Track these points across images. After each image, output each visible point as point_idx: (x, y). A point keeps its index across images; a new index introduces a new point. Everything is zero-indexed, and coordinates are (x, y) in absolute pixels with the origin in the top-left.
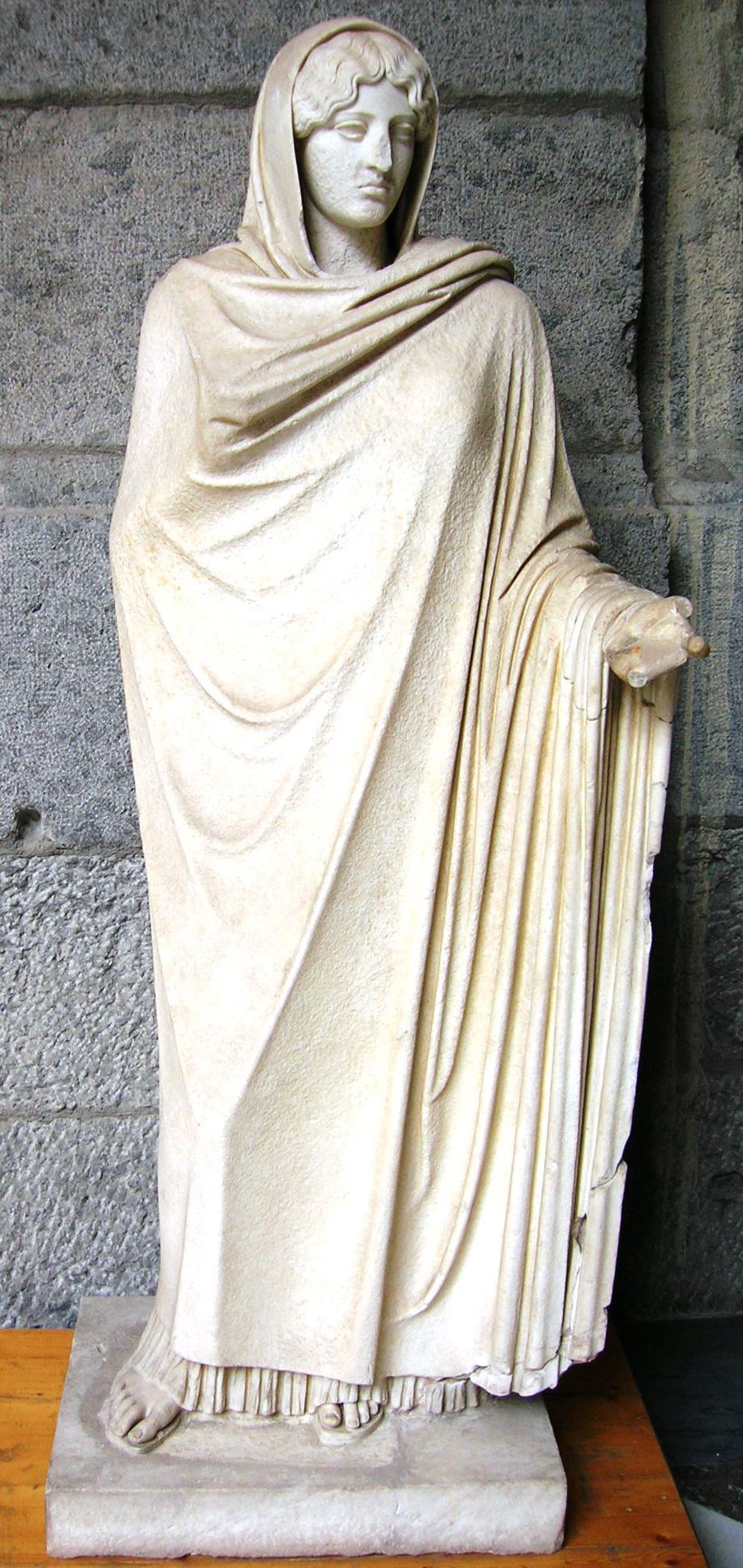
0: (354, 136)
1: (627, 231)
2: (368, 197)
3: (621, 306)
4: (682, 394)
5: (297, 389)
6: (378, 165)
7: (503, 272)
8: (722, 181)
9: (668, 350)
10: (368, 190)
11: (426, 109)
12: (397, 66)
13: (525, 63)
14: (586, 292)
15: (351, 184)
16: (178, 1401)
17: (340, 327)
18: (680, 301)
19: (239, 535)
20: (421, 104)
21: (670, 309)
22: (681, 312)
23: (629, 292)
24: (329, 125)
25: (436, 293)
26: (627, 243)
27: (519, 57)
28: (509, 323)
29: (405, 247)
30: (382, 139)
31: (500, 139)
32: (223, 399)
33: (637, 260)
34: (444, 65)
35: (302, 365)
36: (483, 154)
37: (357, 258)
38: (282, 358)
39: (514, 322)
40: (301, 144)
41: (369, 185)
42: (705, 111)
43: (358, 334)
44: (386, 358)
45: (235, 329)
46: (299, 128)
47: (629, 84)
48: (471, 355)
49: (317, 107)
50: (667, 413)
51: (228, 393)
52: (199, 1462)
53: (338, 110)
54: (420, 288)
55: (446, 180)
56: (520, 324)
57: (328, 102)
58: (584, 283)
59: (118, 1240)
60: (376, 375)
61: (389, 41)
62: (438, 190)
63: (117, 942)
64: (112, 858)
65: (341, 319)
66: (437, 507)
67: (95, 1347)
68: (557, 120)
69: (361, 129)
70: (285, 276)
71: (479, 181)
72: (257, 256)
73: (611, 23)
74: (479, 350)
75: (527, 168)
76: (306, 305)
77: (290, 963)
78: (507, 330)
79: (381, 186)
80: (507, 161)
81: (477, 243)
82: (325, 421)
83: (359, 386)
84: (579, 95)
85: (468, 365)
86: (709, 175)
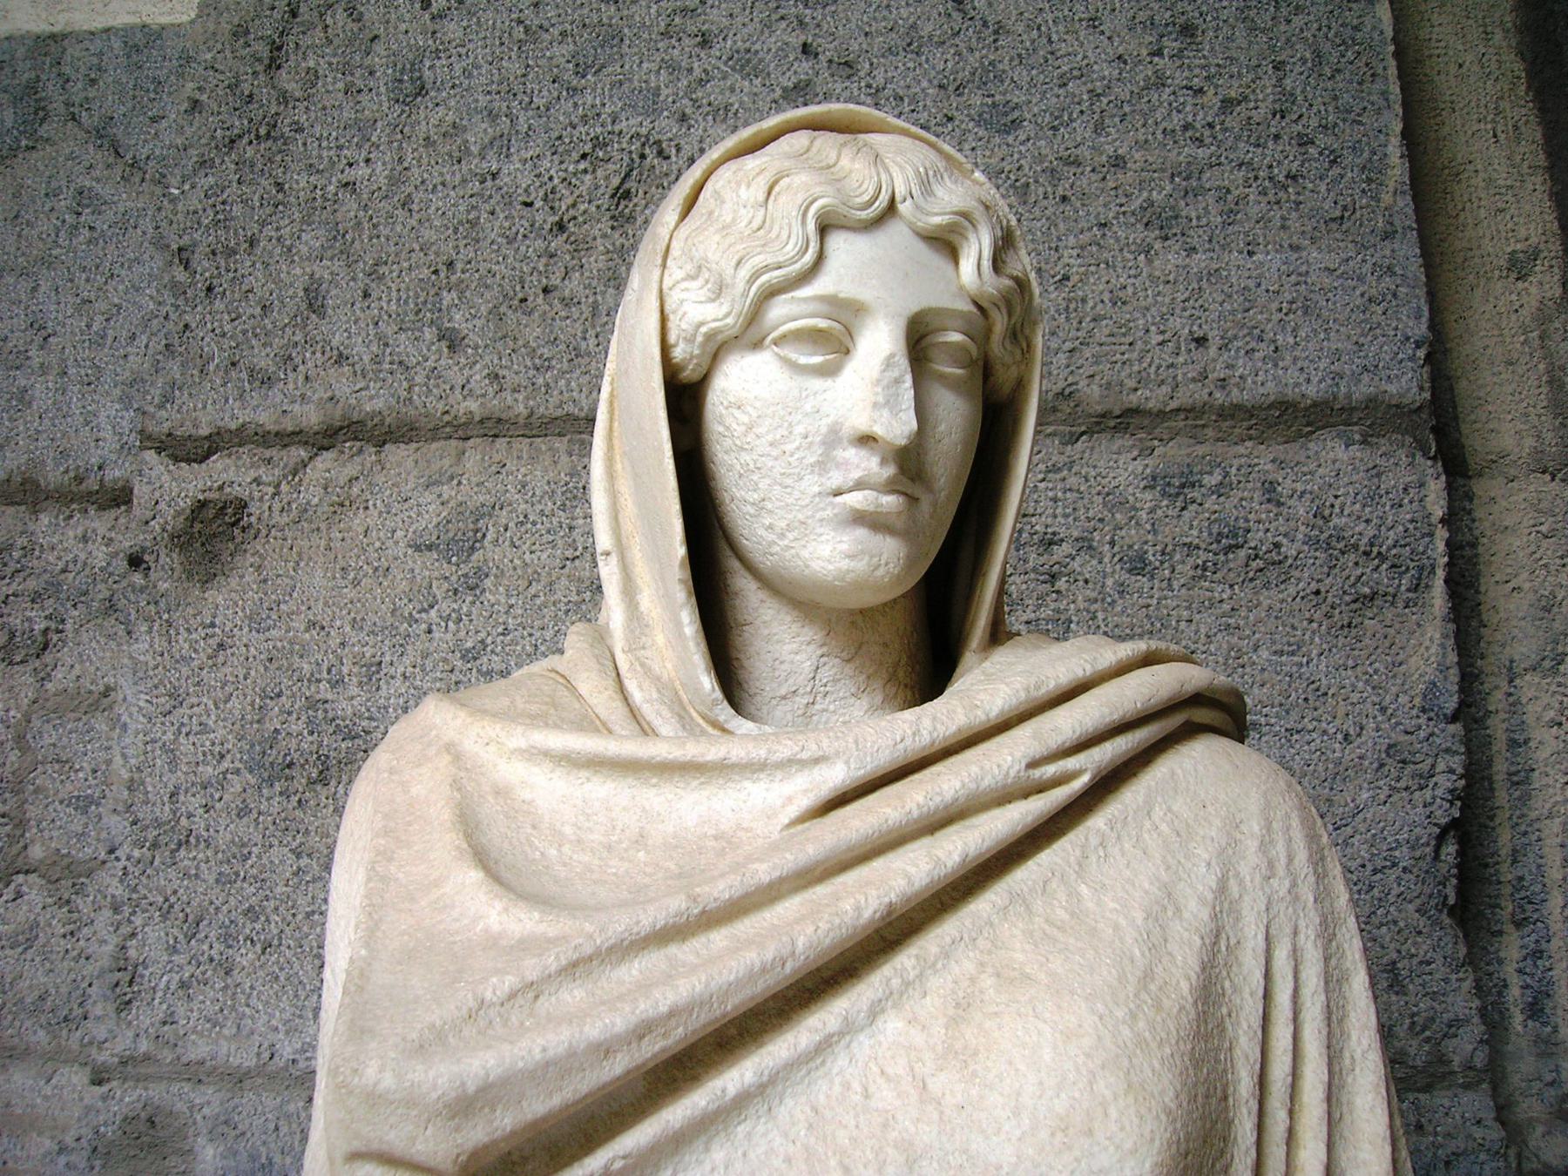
0: (817, 359)
1: (1427, 647)
2: (860, 518)
3: (1428, 793)
4: (1538, 954)
5: (618, 1066)
6: (878, 430)
7: (1215, 714)
9: (1507, 873)
10: (856, 499)
11: (1007, 301)
12: (926, 186)
13: (1213, 351)
14: (1359, 769)
15: (812, 485)
17: (764, 872)
18: (1520, 780)
20: (993, 285)
21: (1502, 796)
22: (1525, 798)
23: (1441, 766)
24: (748, 333)
25: (1050, 770)
26: (1430, 672)
27: (1201, 341)
28: (1252, 845)
29: (969, 658)
30: (889, 363)
31: (1177, 488)
33: (1451, 704)
34: (1062, 358)
35: (644, 987)
36: (1143, 515)
37: (845, 688)
38: (575, 968)
39: (1265, 846)
40: (685, 400)
41: (859, 485)
42: (1529, 442)
43: (821, 891)
44: (905, 961)
45: (475, 875)
46: (678, 353)
47: (1406, 384)
48: (1156, 945)
49: (719, 290)
50: (1514, 992)
51: (388, 1081)
53: (771, 293)
54: (1002, 759)
55: (1075, 565)
56: (1280, 850)
57: (744, 273)
58: (1351, 753)
60: (875, 1012)
61: (906, 142)
62: (1061, 584)
65: (774, 847)
68: (1279, 450)
69: (833, 340)
70: (645, 730)
71: (1138, 565)
72: (593, 689)
73: (1361, 279)
74: (1176, 927)
75: (1230, 539)
76: (688, 809)
78: (1249, 863)
79: (890, 487)
80: (1191, 526)
81: (1154, 644)
82: (718, 1154)
83: (825, 1046)
84: (1315, 405)
85: (1148, 975)
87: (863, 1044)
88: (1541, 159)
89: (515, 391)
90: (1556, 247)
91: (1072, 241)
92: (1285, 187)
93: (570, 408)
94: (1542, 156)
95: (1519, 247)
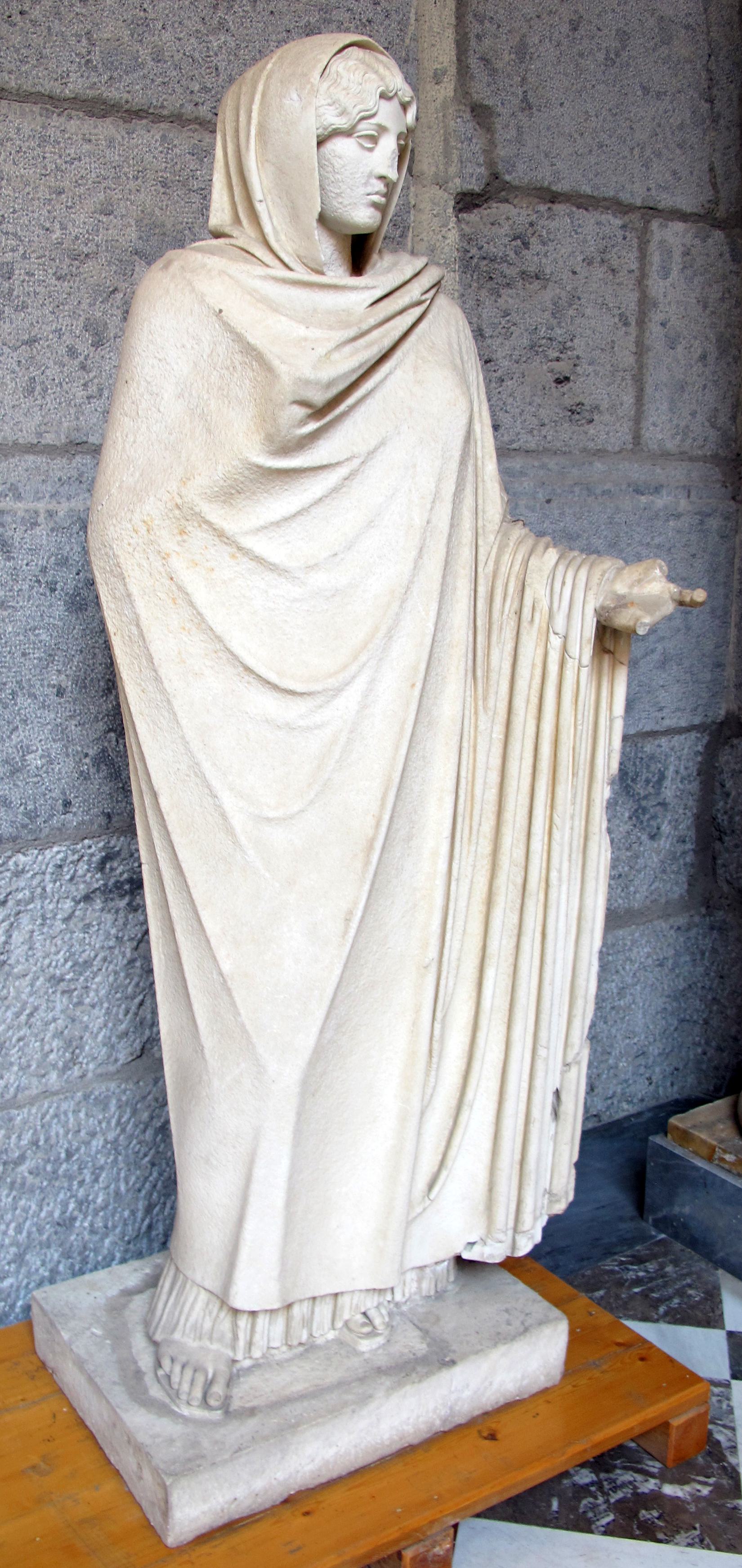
8: (444, 230)
10: (376, 198)
15: (362, 190)
16: (231, 1354)
19: (287, 515)
24: (348, 133)
29: (375, 256)
30: (393, 152)
32: (307, 382)
41: (377, 193)
42: (433, 169)
52: (276, 1405)
57: (356, 110)
59: (19, 1229)
63: (10, 936)
64: (9, 853)
66: (449, 488)
67: (88, 1333)
77: (350, 913)
86: (436, 223)
87: (392, 378)
88: (453, 21)
89: (10, 73)
90: (453, 70)
91: (274, 37)
92: (365, 26)
93: (39, 88)
94: (453, 19)
95: (439, 66)
